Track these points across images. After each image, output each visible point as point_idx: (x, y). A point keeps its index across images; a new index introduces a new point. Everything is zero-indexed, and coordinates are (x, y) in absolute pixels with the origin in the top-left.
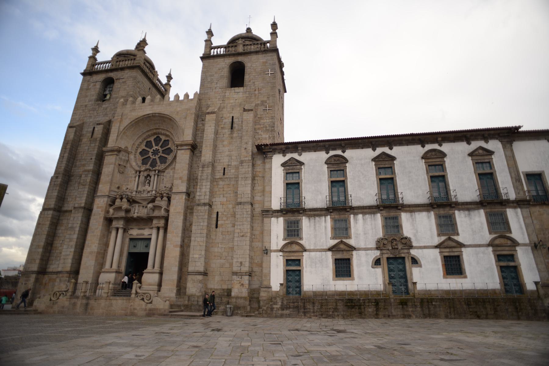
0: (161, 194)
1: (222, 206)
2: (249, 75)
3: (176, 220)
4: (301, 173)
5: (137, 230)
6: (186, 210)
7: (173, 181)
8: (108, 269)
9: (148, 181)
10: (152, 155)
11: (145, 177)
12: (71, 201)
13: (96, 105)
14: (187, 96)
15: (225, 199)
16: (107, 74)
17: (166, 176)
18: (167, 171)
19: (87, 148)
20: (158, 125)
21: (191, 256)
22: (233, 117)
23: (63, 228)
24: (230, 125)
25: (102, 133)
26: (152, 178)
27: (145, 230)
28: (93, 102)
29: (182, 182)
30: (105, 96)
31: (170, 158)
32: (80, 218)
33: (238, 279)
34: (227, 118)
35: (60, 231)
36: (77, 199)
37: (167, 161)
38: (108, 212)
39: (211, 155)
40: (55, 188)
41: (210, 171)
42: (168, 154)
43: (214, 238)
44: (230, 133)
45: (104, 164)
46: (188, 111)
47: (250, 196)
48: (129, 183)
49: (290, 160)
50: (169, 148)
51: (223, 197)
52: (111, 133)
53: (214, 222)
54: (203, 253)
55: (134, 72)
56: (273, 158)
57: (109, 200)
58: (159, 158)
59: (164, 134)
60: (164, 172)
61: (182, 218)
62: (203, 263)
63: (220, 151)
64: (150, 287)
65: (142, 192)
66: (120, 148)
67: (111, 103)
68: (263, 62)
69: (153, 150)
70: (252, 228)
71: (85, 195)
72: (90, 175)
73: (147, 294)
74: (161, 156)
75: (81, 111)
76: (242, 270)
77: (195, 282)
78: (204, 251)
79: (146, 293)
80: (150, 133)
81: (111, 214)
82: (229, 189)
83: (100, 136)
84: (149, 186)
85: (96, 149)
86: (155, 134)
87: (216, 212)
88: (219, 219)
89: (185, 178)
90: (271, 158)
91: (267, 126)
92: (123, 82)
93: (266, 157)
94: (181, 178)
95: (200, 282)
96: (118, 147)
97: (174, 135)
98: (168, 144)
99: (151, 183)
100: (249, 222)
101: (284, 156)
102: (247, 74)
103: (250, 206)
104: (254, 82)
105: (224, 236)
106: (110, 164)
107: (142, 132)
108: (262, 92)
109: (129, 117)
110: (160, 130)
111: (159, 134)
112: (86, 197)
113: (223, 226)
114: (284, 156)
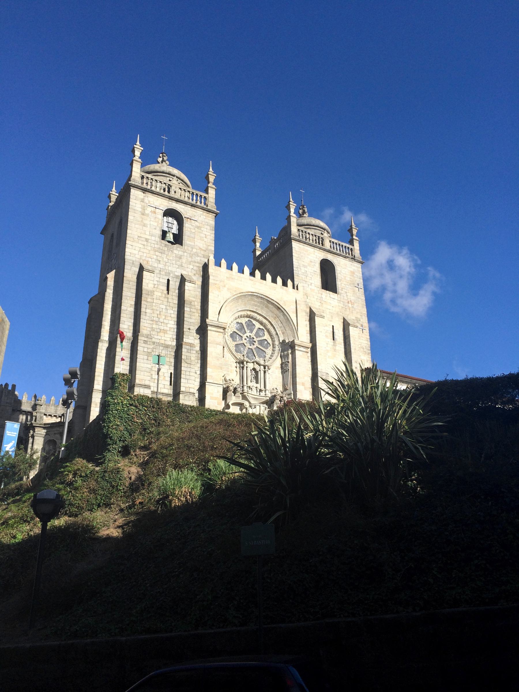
2: (340, 281)
13: (163, 245)
16: (170, 202)
19: (164, 307)
22: (333, 326)
26: (261, 375)
40: (146, 357)
44: (332, 344)
55: (209, 218)
59: (258, 321)
65: (253, 389)
75: (142, 246)
80: (243, 313)
91: (364, 347)
92: (198, 227)
94: (303, 384)
102: (339, 280)
104: (346, 292)
106: (217, 344)
107: (237, 309)
111: (252, 318)
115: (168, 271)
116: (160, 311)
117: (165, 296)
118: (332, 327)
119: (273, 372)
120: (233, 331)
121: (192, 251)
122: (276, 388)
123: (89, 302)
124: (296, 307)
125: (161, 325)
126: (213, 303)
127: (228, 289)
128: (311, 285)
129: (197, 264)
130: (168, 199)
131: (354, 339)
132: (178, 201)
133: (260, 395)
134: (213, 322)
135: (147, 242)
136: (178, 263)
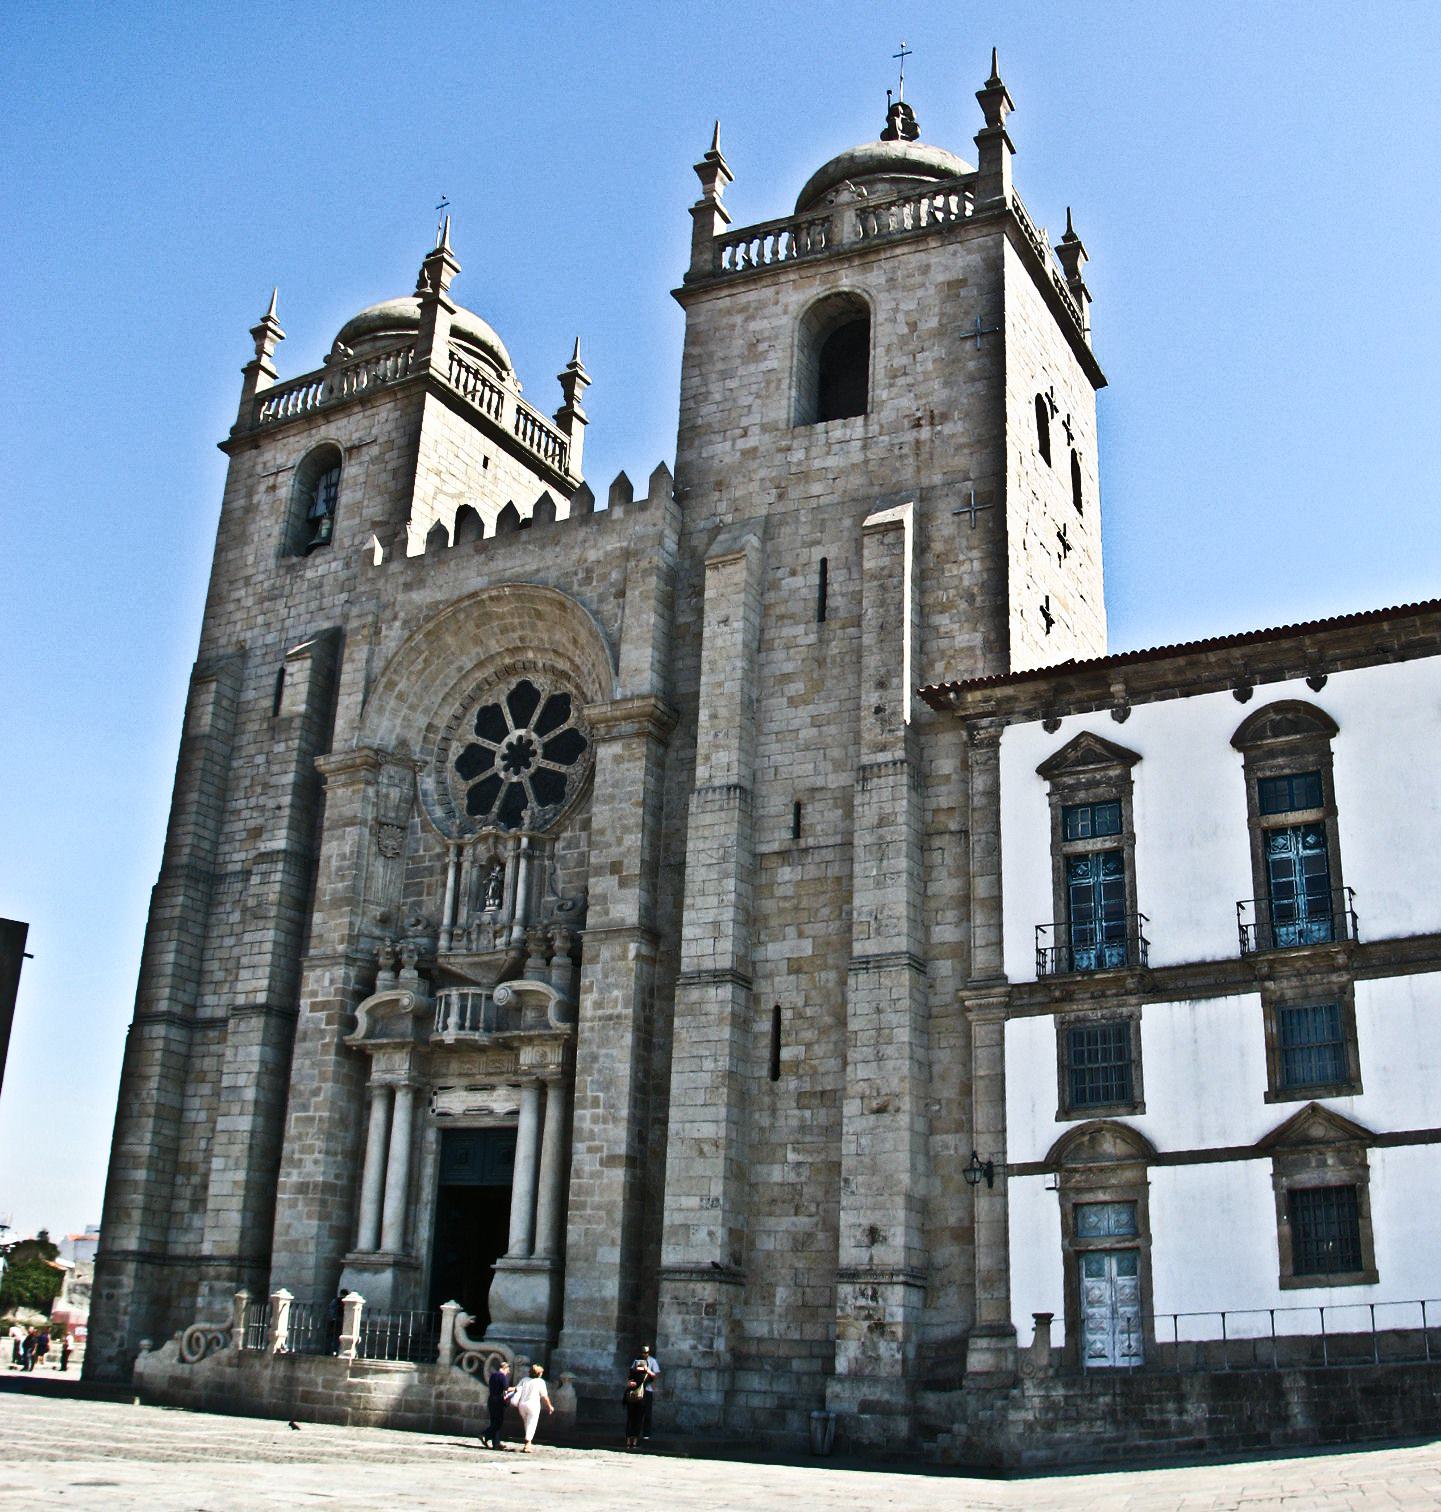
0: (549, 942)
1: (792, 977)
3: (603, 1051)
4: (1130, 802)
5: (465, 1093)
6: (644, 1005)
7: (587, 880)
8: (368, 1253)
9: (493, 884)
10: (506, 769)
11: (481, 866)
12: (226, 981)
13: (282, 572)
14: (622, 488)
15: (807, 948)
16: (314, 431)
17: (564, 857)
18: (567, 834)
20: (516, 635)
21: (669, 1201)
22: (824, 562)
23: (206, 1089)
24: (813, 605)
25: (311, 693)
26: (509, 870)
27: (495, 1093)
28: (272, 563)
29: (623, 884)
30: (314, 523)
31: (573, 771)
32: (256, 1051)
33: (862, 1302)
34: (799, 568)
35: (196, 1102)
36: (244, 974)
37: (567, 789)
38: (350, 1024)
39: (734, 756)
41: (733, 829)
42: (569, 760)
43: (766, 1122)
44: (812, 638)
45: (326, 824)
46: (628, 560)
47: (904, 926)
48: (424, 898)
49: (1074, 744)
50: (572, 732)
51: (801, 935)
52: (342, 690)
53: (766, 1053)
54: (717, 1189)
56: (1001, 740)
57: (353, 973)
58: (532, 778)
60: (557, 838)
61: (628, 1039)
62: (720, 1233)
63: (774, 727)
64: (522, 1327)
65: (474, 936)
66: (377, 751)
67: (335, 559)
68: (949, 284)
69: (510, 746)
70: (925, 1072)
71: (268, 957)
72: (278, 876)
73: (492, 1356)
74: (539, 768)
76: (875, 1262)
77: (687, 1313)
78: (721, 1182)
79: (491, 1352)
80: (489, 671)
81: (362, 1034)
82: (823, 899)
83: (302, 708)
84: (500, 906)
85: (293, 767)
86: (509, 671)
87: (771, 1006)
88: (783, 1042)
89: (633, 866)
90: (994, 744)
93: (971, 737)
94: (615, 868)
95: (707, 1314)
96: (370, 748)
97: (586, 671)
99: (507, 895)
100: (907, 1048)
101: (1052, 726)
103: (906, 976)
104: (913, 385)
105: (808, 1113)
106: (347, 825)
107: (460, 669)
108: (947, 429)
109: (402, 615)
112: (272, 965)
113: (801, 1072)
114: (1052, 726)
118: (817, 567)
119: (568, 847)
120: (467, 743)
126: (350, 694)
127: (405, 622)
130: (306, 426)
136: (313, 605)
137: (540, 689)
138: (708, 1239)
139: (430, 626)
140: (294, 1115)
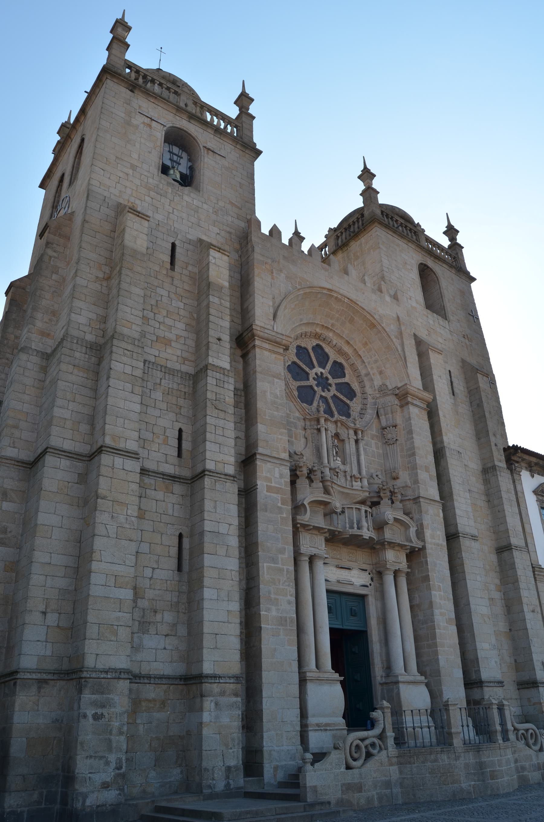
5: (335, 569)
10: (317, 385)
20: (331, 321)
22: (450, 371)
26: (350, 447)
40: (129, 386)
44: (453, 401)
50: (347, 384)
58: (332, 397)
65: (339, 476)
67: (205, 203)
80: (308, 329)
93: (515, 470)
94: (427, 469)
98: (344, 376)
106: (274, 377)
107: (301, 320)
110: (331, 335)
115: (173, 227)
116: (157, 301)
117: (167, 273)
121: (217, 204)
122: (377, 476)
123: (7, 293)
124: (400, 329)
125: (159, 328)
128: (410, 299)
129: (225, 227)
130: (174, 111)
131: (486, 395)
132: (192, 117)
133: (354, 488)
134: (266, 331)
135: (133, 170)
137: (329, 354)
138: (495, 665)
139: (308, 290)
140: (265, 564)
